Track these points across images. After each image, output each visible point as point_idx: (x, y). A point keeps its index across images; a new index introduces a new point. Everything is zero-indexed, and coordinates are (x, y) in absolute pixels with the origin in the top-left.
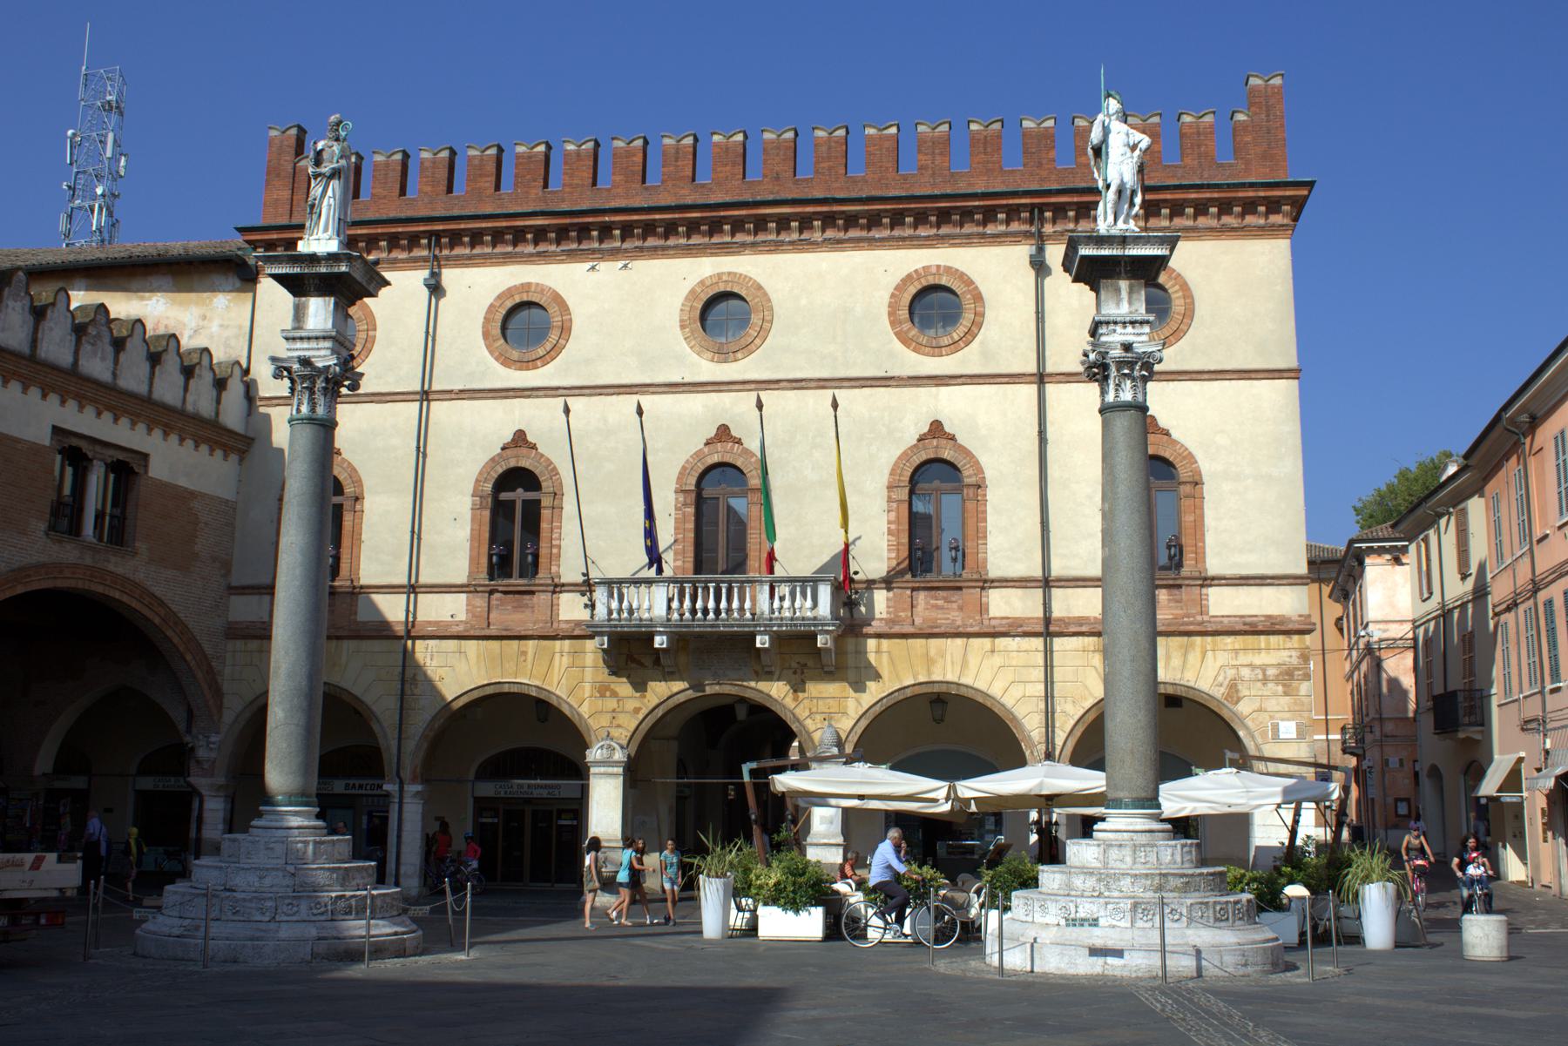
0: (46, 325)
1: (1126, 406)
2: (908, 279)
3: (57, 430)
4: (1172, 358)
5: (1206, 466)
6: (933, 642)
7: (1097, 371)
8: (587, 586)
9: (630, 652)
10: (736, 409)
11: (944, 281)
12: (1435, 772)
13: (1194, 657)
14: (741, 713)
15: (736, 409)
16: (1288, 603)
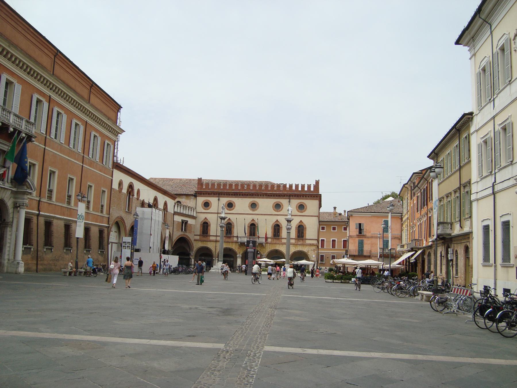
5: (307, 226)
8: (237, 237)
9: (242, 244)
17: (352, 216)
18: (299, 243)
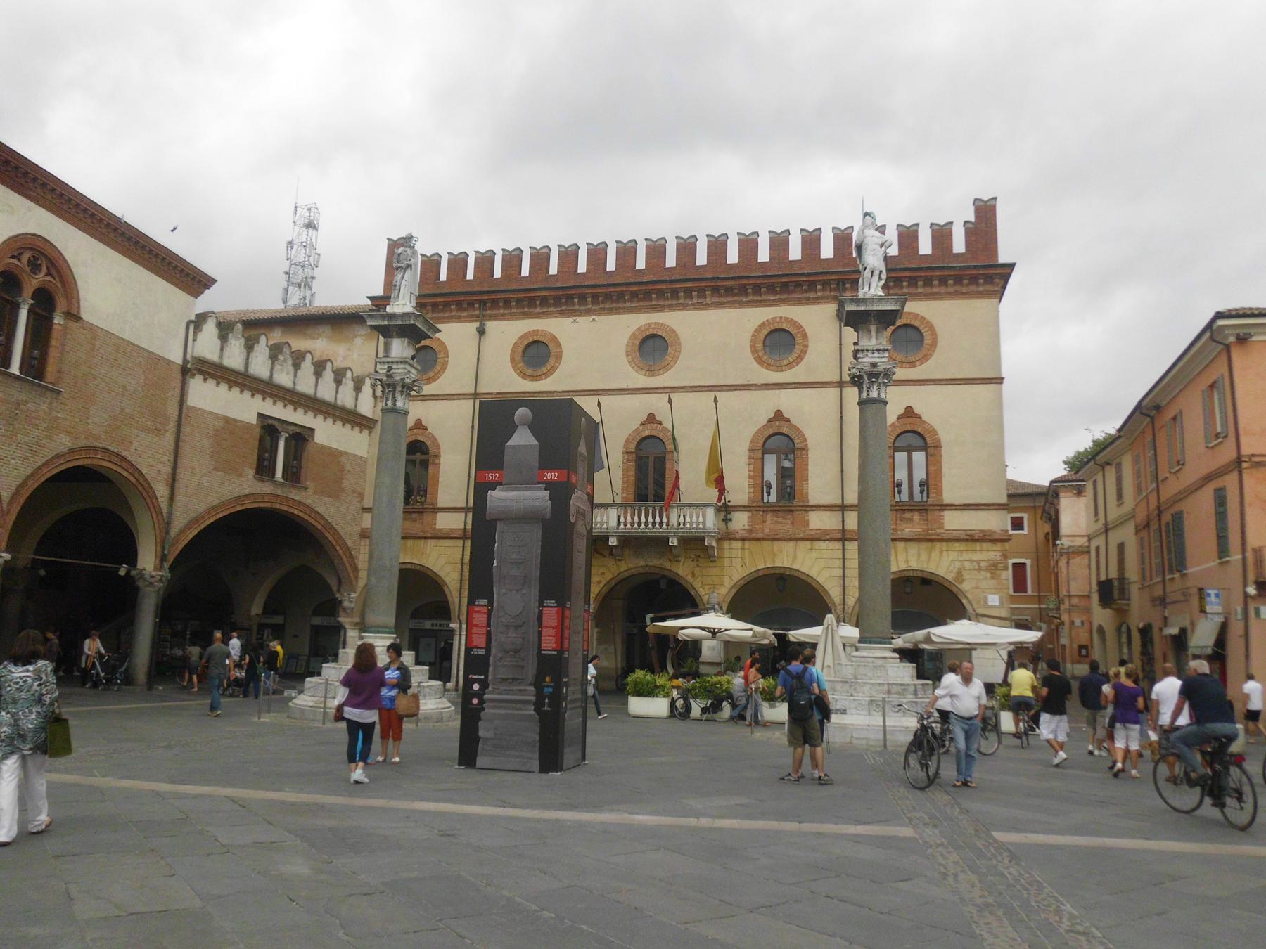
0: (253, 355)
1: (874, 401)
2: (762, 325)
3: (260, 415)
4: (900, 373)
5: (944, 437)
6: (777, 544)
7: (857, 381)
10: (657, 404)
11: (784, 326)
12: (1101, 630)
13: (935, 554)
14: (663, 585)
15: (657, 404)
16: (997, 522)
17: (1242, 340)
18: (907, 530)
